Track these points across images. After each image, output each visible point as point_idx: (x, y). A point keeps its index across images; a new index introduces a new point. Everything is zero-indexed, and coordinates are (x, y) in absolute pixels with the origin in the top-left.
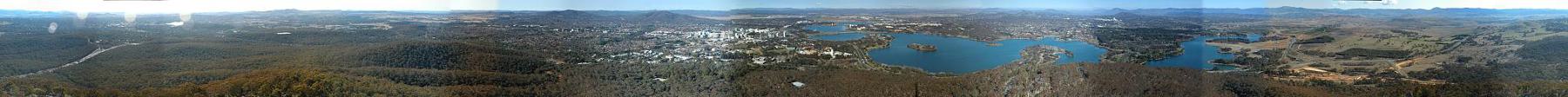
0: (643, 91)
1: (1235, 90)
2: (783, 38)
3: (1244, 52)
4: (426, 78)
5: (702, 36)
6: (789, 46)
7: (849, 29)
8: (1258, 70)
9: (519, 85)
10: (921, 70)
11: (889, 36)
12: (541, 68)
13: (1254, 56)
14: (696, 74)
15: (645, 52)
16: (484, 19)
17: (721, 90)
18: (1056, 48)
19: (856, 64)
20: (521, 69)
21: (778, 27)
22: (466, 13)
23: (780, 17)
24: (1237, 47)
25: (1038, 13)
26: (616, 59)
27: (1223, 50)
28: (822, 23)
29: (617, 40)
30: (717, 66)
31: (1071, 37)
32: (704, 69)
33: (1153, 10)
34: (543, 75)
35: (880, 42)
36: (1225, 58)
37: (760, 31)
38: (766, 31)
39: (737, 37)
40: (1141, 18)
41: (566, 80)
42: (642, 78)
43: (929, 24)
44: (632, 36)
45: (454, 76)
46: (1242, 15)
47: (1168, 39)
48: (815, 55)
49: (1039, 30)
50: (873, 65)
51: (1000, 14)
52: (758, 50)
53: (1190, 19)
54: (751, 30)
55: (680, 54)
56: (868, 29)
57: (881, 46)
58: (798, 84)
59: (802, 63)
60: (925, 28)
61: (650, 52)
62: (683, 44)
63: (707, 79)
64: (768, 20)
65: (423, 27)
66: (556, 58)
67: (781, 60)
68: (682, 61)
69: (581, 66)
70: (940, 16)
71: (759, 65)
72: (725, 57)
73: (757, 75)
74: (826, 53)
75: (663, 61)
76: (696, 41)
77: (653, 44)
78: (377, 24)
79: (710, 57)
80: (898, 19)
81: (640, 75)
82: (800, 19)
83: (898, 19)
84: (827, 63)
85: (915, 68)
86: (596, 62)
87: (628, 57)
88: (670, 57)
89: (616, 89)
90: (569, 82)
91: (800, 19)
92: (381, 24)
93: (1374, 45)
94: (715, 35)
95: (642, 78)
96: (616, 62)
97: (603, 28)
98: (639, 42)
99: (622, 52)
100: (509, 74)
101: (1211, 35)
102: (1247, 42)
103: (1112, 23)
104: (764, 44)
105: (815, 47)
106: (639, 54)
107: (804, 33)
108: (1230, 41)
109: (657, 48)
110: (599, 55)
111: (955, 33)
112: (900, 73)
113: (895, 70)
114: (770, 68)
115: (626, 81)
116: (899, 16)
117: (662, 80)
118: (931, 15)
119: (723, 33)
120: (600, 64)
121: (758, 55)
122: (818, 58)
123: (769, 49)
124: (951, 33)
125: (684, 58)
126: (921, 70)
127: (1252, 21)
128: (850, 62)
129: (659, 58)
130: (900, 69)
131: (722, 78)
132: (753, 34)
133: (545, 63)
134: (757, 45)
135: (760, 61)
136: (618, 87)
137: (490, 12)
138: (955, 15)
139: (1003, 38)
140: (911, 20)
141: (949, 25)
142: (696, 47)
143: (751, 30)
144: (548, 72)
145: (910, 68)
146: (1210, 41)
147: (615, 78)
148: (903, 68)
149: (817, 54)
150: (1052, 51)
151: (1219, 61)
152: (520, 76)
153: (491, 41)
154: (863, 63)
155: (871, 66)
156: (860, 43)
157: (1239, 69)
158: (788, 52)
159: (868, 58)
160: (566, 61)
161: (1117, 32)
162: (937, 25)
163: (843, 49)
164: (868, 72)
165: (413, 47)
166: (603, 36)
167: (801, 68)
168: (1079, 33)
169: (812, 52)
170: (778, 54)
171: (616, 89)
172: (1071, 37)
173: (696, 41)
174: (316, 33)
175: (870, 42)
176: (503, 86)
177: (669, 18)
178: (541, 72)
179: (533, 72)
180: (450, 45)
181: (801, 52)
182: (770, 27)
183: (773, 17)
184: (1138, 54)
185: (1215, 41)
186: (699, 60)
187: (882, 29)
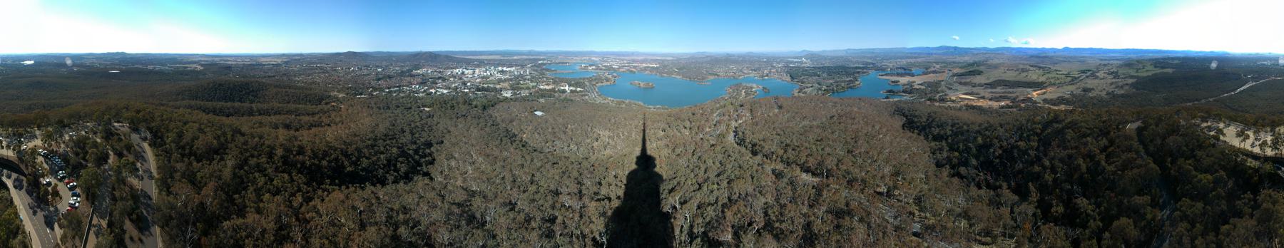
1: (904, 115)
3: (910, 84)
4: (231, 110)
5: (459, 73)
6: (532, 81)
7: (582, 69)
8: (922, 98)
9: (309, 115)
10: (642, 104)
11: (615, 74)
12: (327, 101)
13: (918, 87)
16: (279, 61)
17: (475, 117)
18: (755, 86)
19: (587, 97)
20: (310, 101)
21: (523, 66)
22: (264, 56)
23: (525, 57)
24: (904, 80)
25: (740, 56)
27: (892, 82)
28: (559, 63)
29: (390, 77)
30: (472, 97)
31: (767, 75)
32: (461, 100)
33: (834, 51)
34: (329, 106)
35: (608, 80)
36: (895, 89)
37: (508, 69)
38: (512, 69)
39: (489, 74)
40: (825, 58)
42: (411, 108)
43: (649, 65)
44: (402, 74)
45: (255, 109)
46: (907, 53)
47: (848, 74)
48: (553, 90)
49: (741, 71)
50: (601, 99)
51: (707, 57)
52: (506, 85)
53: (864, 57)
54: (500, 69)
55: (441, 88)
56: (598, 68)
57: (609, 83)
58: (539, 113)
59: (543, 96)
60: (646, 68)
61: (417, 86)
62: (444, 79)
63: (464, 108)
64: (515, 60)
65: (229, 68)
66: (339, 91)
67: (524, 93)
68: (443, 94)
69: (359, 98)
70: (659, 58)
71: (507, 98)
72: (478, 90)
73: (505, 105)
74: (562, 88)
75: (428, 94)
76: (455, 77)
77: (419, 80)
78: (191, 65)
79: (466, 90)
80: (623, 60)
81: (409, 105)
82: (540, 60)
83: (623, 60)
84: (563, 96)
85: (637, 102)
86: (372, 95)
87: (399, 91)
88: (433, 91)
89: (390, 117)
90: (350, 111)
91: (540, 60)
92: (195, 66)
93: (1015, 77)
94: (471, 71)
95: (411, 108)
97: (377, 67)
98: (408, 79)
100: (300, 106)
101: (883, 70)
102: (913, 75)
103: (802, 63)
104: (511, 80)
105: (554, 83)
107: (544, 71)
108: (898, 75)
109: (423, 83)
110: (375, 89)
111: (670, 73)
112: (624, 106)
113: (620, 103)
114: (516, 100)
115: (398, 111)
116: (623, 58)
117: (427, 109)
118: (650, 58)
119: (477, 70)
120: (376, 96)
121: (506, 89)
122: (556, 92)
123: (515, 84)
124: (666, 73)
125: (445, 91)
126: (642, 104)
127: (915, 58)
129: (425, 91)
130: (624, 102)
131: (476, 107)
132: (502, 72)
133: (330, 96)
134: (505, 80)
135: (508, 94)
136: (391, 115)
137: (284, 55)
138: (671, 59)
140: (634, 61)
141: (665, 67)
142: (455, 82)
143: (500, 69)
144: (333, 104)
145: (632, 101)
146: (882, 75)
147: (389, 108)
148: (627, 102)
150: (752, 88)
151: (890, 91)
152: (309, 107)
153: (285, 78)
154: (594, 97)
155: (599, 100)
156: (590, 80)
157: (906, 97)
158: (531, 87)
160: (347, 94)
161: (806, 70)
162: (655, 66)
163: (577, 84)
164: (597, 104)
165: (220, 85)
166: (378, 73)
167: (542, 100)
168: (774, 72)
169: (551, 87)
170: (523, 88)
171: (390, 117)
172: (767, 75)
173: (455, 77)
174: (161, 73)
175: (599, 79)
176: (296, 116)
177: (432, 58)
178: (327, 104)
179: (320, 104)
180: (251, 83)
181: (542, 87)
182: (516, 65)
183: (519, 57)
184: (824, 87)
185: (886, 75)
186: (457, 93)
187: (609, 69)
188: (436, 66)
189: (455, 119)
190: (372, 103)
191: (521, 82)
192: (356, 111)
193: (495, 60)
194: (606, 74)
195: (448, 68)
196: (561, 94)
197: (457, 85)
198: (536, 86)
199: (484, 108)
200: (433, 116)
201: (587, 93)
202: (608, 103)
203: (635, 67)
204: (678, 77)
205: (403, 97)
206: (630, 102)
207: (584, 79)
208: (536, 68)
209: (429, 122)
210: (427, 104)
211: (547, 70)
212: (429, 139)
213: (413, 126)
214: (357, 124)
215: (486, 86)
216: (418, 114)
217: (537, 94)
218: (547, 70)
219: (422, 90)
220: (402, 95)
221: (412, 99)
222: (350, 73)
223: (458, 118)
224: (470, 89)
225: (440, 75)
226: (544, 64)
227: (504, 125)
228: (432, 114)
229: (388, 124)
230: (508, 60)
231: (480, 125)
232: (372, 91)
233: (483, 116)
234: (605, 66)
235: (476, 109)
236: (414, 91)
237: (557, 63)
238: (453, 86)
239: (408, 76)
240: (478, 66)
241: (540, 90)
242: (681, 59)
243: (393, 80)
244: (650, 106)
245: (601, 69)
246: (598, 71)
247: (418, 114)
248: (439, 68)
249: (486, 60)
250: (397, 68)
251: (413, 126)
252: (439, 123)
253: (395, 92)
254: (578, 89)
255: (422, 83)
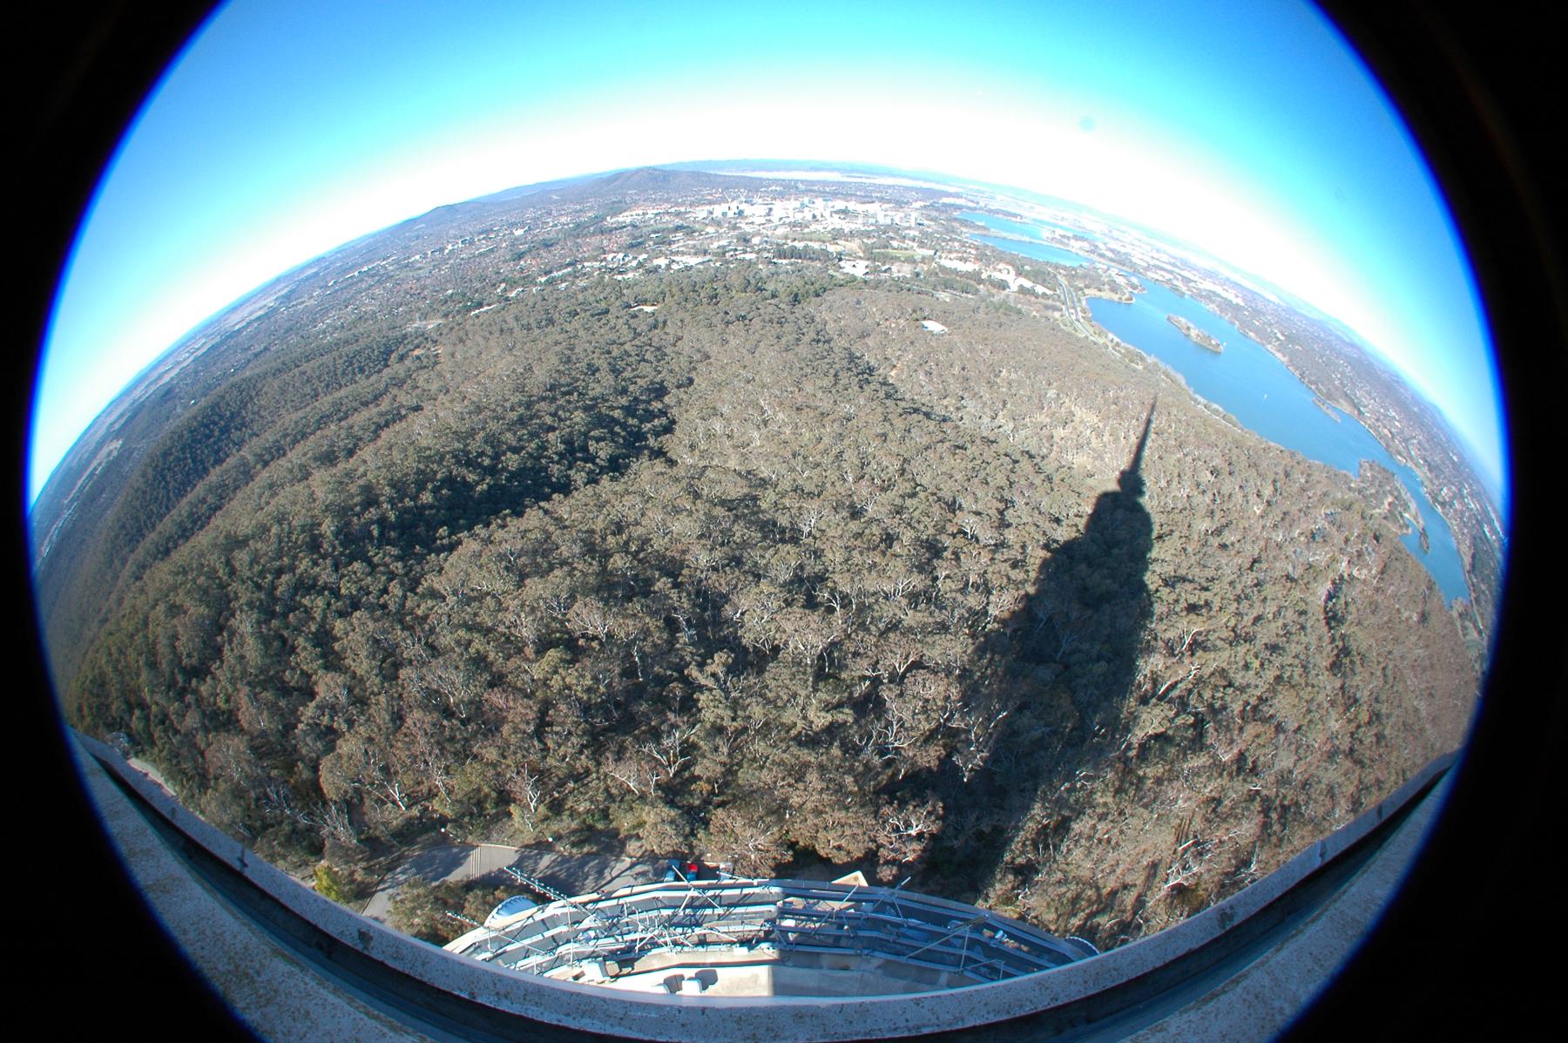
0: (613, 336)
2: (909, 228)
5: (730, 214)
6: (922, 245)
9: (366, 404)
10: (1183, 382)
11: (1135, 280)
12: (402, 350)
14: (720, 291)
15: (610, 257)
17: (771, 321)
19: (1057, 315)
20: (362, 370)
21: (899, 204)
26: (550, 282)
28: (997, 212)
29: (547, 245)
30: (764, 273)
32: (735, 280)
34: (407, 362)
35: (1114, 288)
39: (809, 217)
41: (453, 355)
42: (607, 312)
43: (1218, 290)
44: (579, 230)
50: (1091, 330)
51: (1352, 345)
52: (854, 245)
55: (683, 253)
56: (1094, 250)
57: (1115, 297)
58: (934, 326)
59: (947, 286)
60: (1210, 296)
61: (621, 256)
62: (690, 231)
63: (742, 301)
66: (425, 316)
67: (902, 271)
69: (477, 317)
71: (854, 279)
72: (782, 254)
73: (850, 296)
75: (649, 272)
76: (718, 224)
77: (625, 239)
79: (748, 256)
81: (603, 305)
82: (949, 195)
83: (1158, 251)
84: (1000, 296)
85: (1172, 373)
86: (507, 299)
88: (662, 262)
89: (557, 343)
90: (459, 356)
94: (763, 210)
95: (607, 312)
96: (550, 288)
97: (513, 225)
98: (595, 241)
99: (561, 267)
100: (343, 392)
104: (868, 234)
105: (978, 259)
106: (597, 264)
107: (956, 224)
109: (636, 246)
110: (513, 284)
113: (1134, 357)
114: (878, 285)
115: (576, 323)
117: (648, 309)
120: (518, 300)
121: (853, 256)
123: (879, 247)
125: (693, 261)
126: (1183, 382)
128: (1047, 307)
129: (640, 265)
130: (1142, 359)
131: (774, 296)
132: (845, 212)
133: (405, 337)
135: (859, 269)
136: (560, 338)
138: (1273, 298)
139: (1345, 407)
141: (1257, 313)
142: (719, 237)
144: (416, 352)
145: (1162, 365)
147: (551, 322)
149: (979, 273)
152: (364, 385)
154: (1073, 319)
155: (1084, 331)
156: (1072, 274)
158: (918, 258)
159: (1084, 311)
160: (446, 316)
162: (1235, 301)
163: (1039, 275)
164: (1078, 340)
166: (515, 242)
167: (945, 296)
169: (969, 267)
170: (897, 259)
171: (557, 343)
173: (718, 224)
175: (1093, 280)
176: (340, 420)
177: (657, 181)
178: (402, 358)
179: (387, 366)
182: (882, 200)
186: (727, 262)
187: (1122, 260)
188: (667, 201)
189: (720, 327)
190: (510, 319)
191: (895, 244)
192: (473, 352)
193: (825, 183)
194: (1113, 272)
195: (700, 203)
196: (994, 291)
197: (724, 242)
198: (932, 259)
199: (796, 299)
200: (665, 322)
201: (1058, 304)
202: (1107, 347)
203: (1186, 280)
204: (1279, 355)
205: (585, 289)
206: (1155, 365)
207: (1057, 267)
208: (934, 214)
209: (656, 339)
210: (648, 296)
211: (964, 223)
212: (658, 379)
213: (616, 352)
214: (479, 383)
215: (800, 245)
216: (627, 323)
217: (933, 279)
218: (964, 223)
219: (634, 263)
220: (582, 283)
221: (608, 290)
222: (445, 261)
223: (728, 323)
224: (758, 252)
225: (678, 222)
226: (959, 208)
227: (844, 343)
228: (661, 319)
229: (554, 360)
230: (860, 186)
231: (784, 340)
232: (505, 290)
233: (791, 318)
234: (1112, 251)
235: (772, 301)
236: (612, 269)
237: (990, 211)
238: (716, 245)
239: (593, 234)
240: (781, 196)
241: (943, 269)
242: (1296, 313)
243: (557, 250)
244: (1200, 399)
245: (1102, 256)
246: (1095, 257)
247: (627, 323)
248: (677, 204)
249: (802, 182)
250: (563, 220)
251: (616, 352)
252: (680, 339)
253: (563, 281)
254: (1040, 289)
255: (632, 246)
